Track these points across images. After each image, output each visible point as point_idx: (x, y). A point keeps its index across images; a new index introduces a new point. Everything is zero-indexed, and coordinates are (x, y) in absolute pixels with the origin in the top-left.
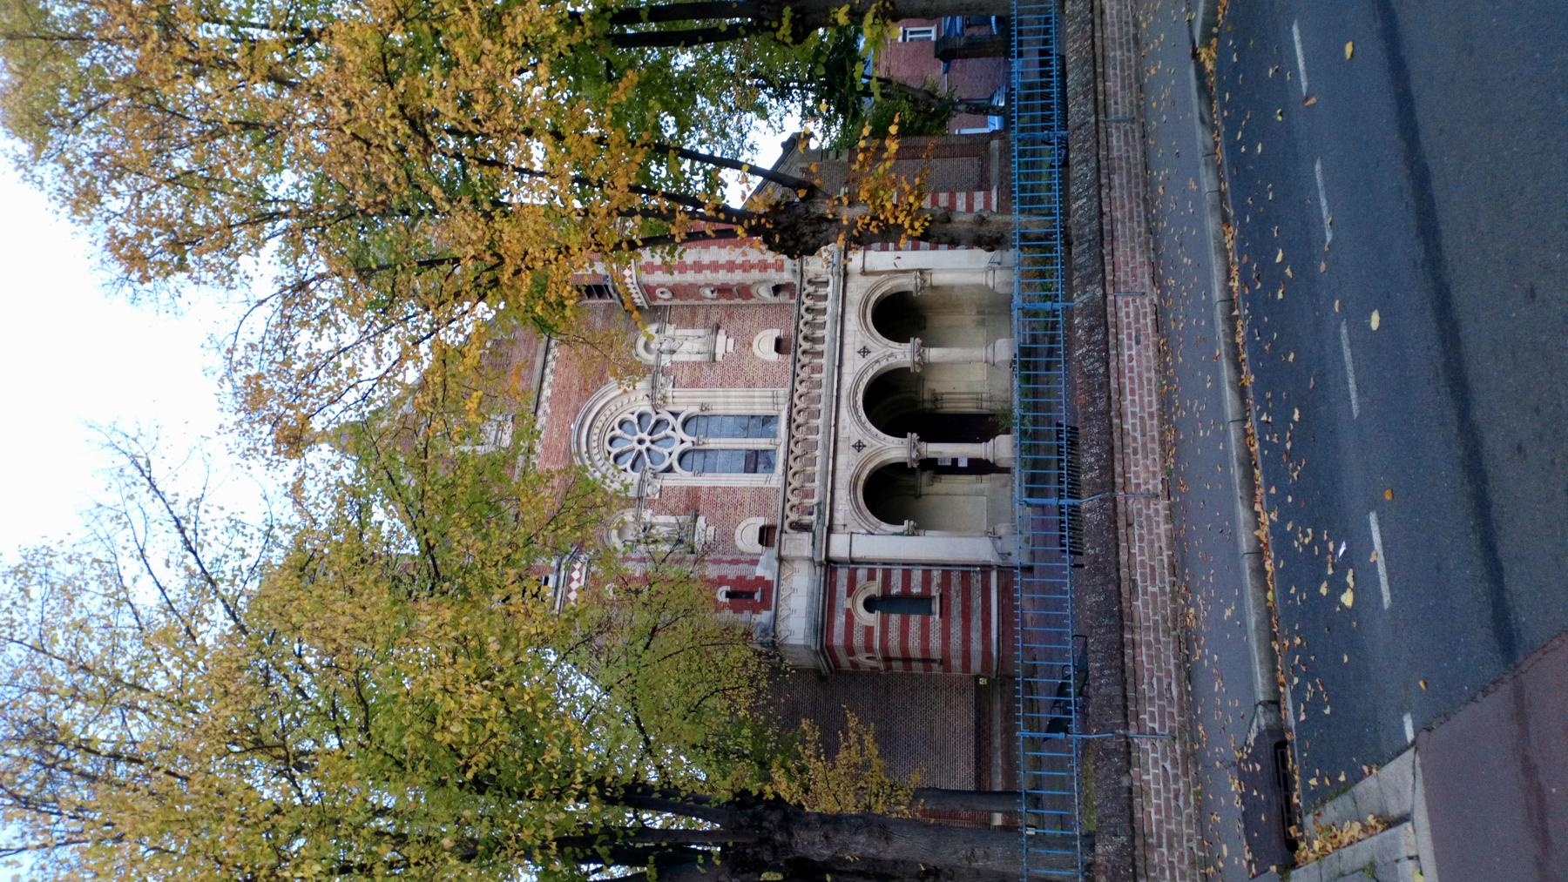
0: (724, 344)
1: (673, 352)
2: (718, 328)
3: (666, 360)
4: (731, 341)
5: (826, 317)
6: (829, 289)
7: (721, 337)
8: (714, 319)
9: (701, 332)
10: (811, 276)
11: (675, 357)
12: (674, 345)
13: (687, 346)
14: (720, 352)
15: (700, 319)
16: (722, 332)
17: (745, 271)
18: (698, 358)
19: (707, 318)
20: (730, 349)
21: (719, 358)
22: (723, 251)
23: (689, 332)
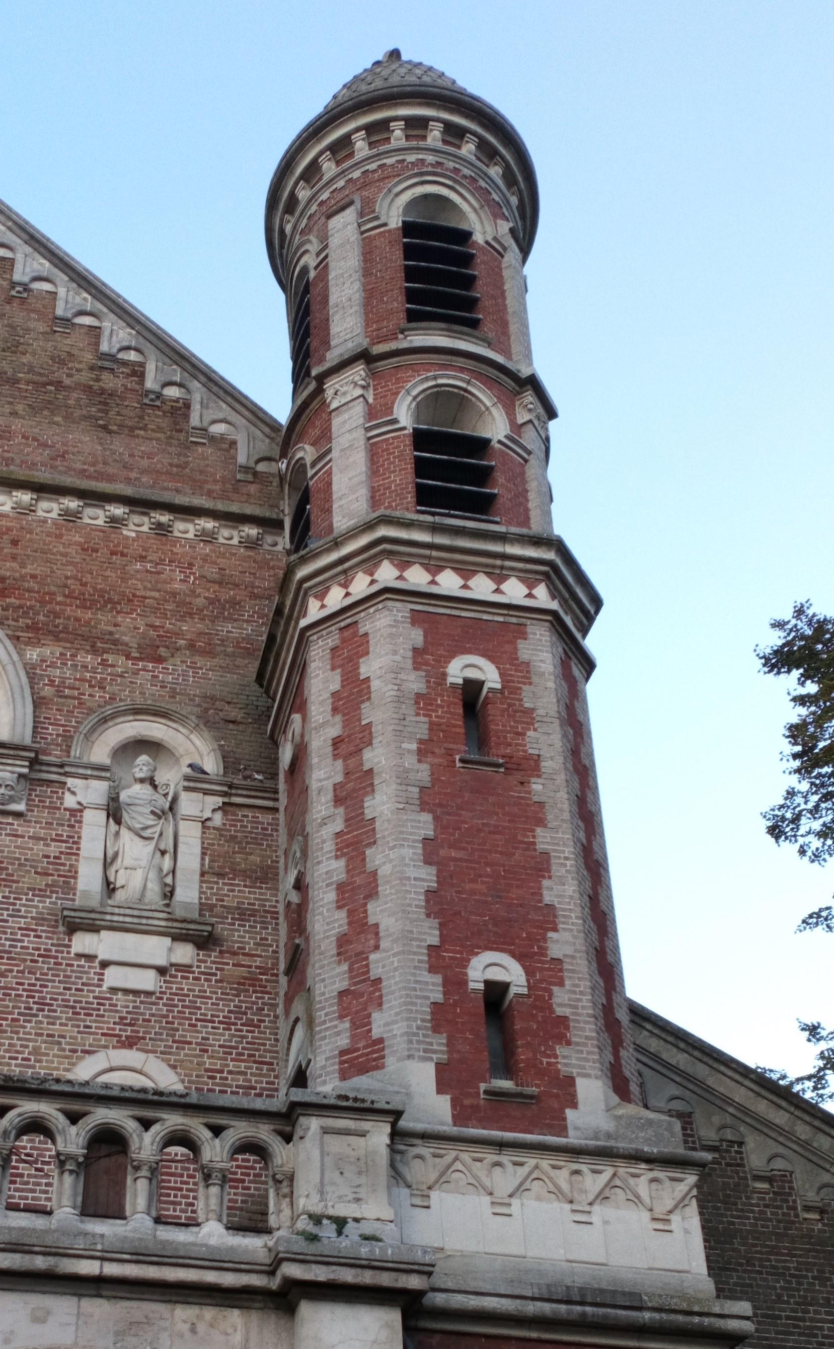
0: (134, 958)
1: (114, 811)
2: (205, 941)
3: (87, 793)
4: (147, 981)
5: (65, 1213)
6: (213, 1234)
7: (156, 949)
8: (238, 935)
9: (188, 893)
10: (281, 1153)
11: (94, 823)
12: (138, 817)
13: (135, 852)
14: (104, 944)
15: (240, 893)
16: (185, 953)
17: (343, 941)
18: (89, 879)
19: (244, 914)
20: (114, 977)
21: (82, 942)
22: (412, 852)
23: (190, 857)
